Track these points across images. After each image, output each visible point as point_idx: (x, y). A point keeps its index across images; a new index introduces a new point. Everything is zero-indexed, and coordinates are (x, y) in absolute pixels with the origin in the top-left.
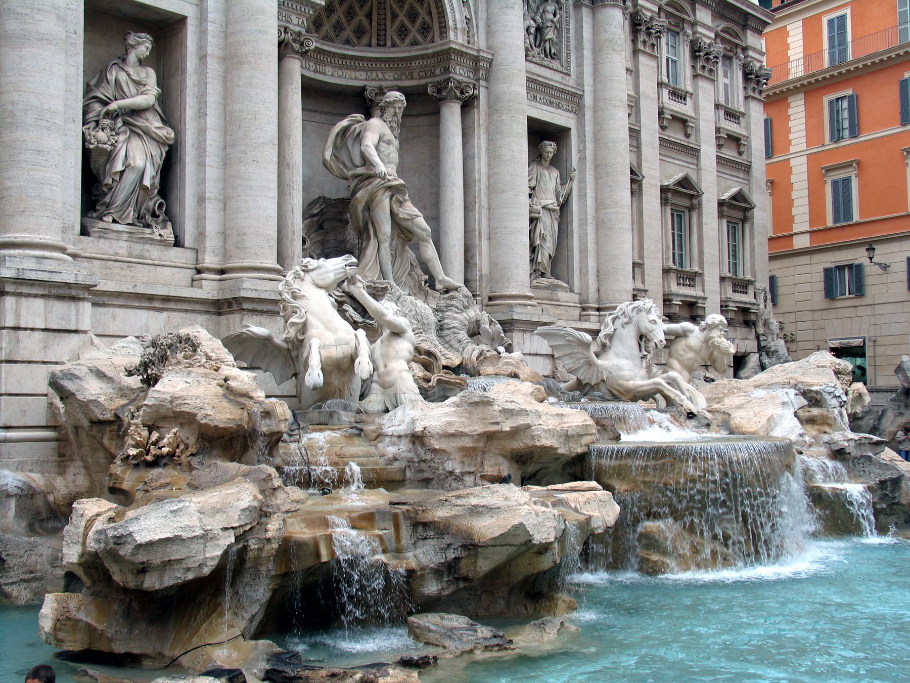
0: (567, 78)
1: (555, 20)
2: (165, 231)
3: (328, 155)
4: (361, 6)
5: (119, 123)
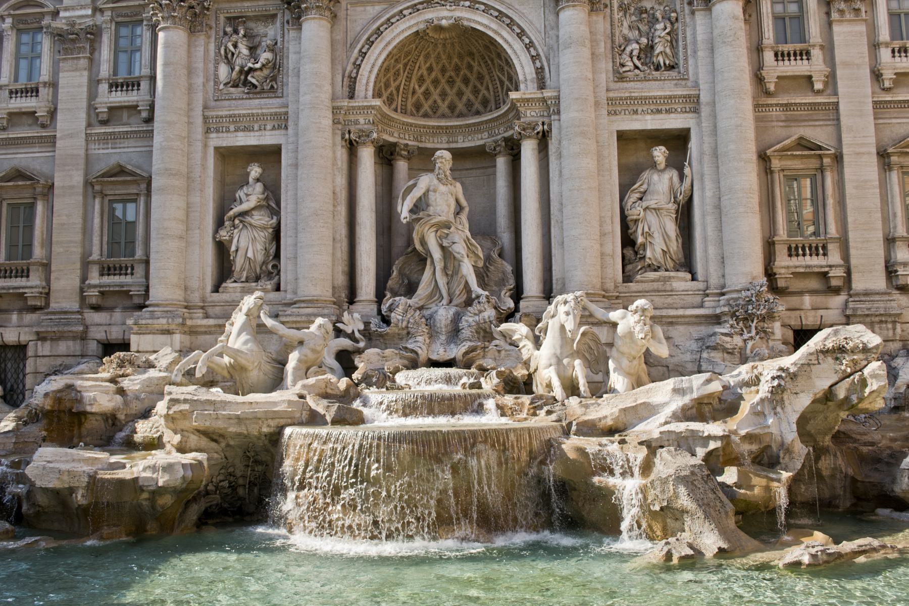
0: (683, 82)
2: (268, 283)
4: (482, 83)
5: (237, 222)
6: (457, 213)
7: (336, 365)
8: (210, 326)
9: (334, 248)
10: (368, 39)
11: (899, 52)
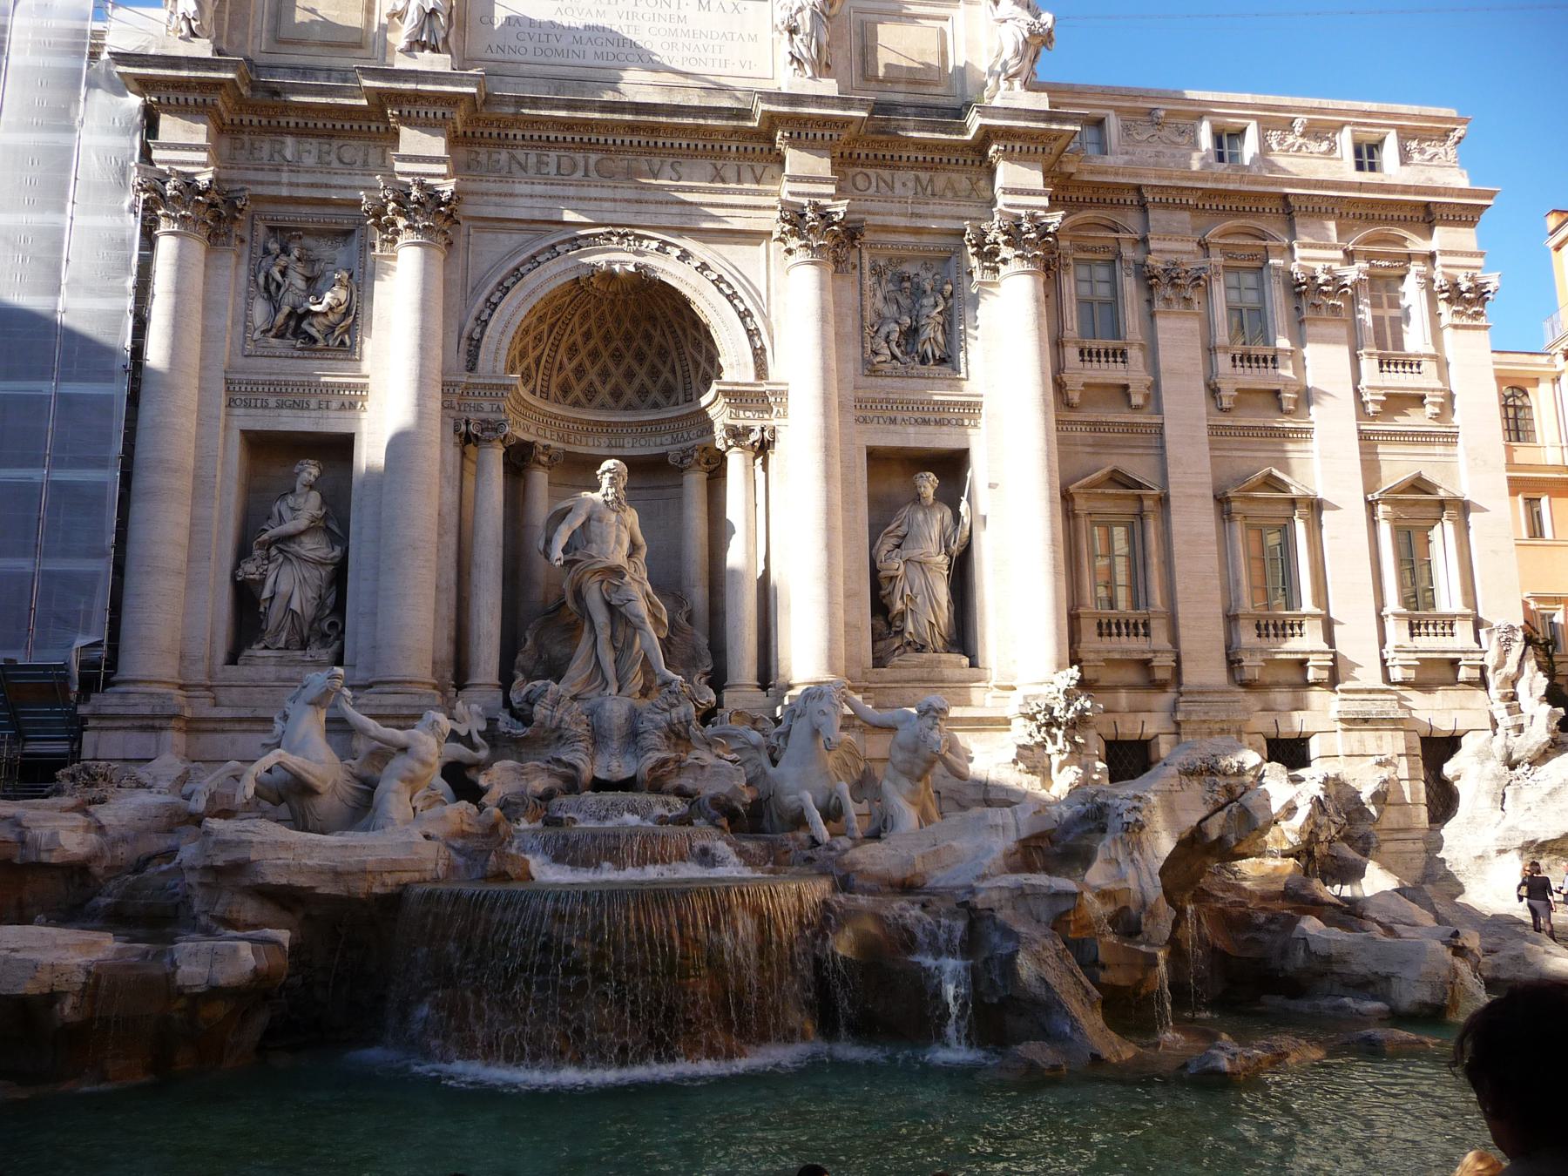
1: (934, 313)
2: (323, 651)
3: (541, 545)
5: (274, 551)
6: (630, 556)
7: (442, 786)
8: (222, 720)
9: (437, 601)
10: (501, 283)
11: (1241, 360)
